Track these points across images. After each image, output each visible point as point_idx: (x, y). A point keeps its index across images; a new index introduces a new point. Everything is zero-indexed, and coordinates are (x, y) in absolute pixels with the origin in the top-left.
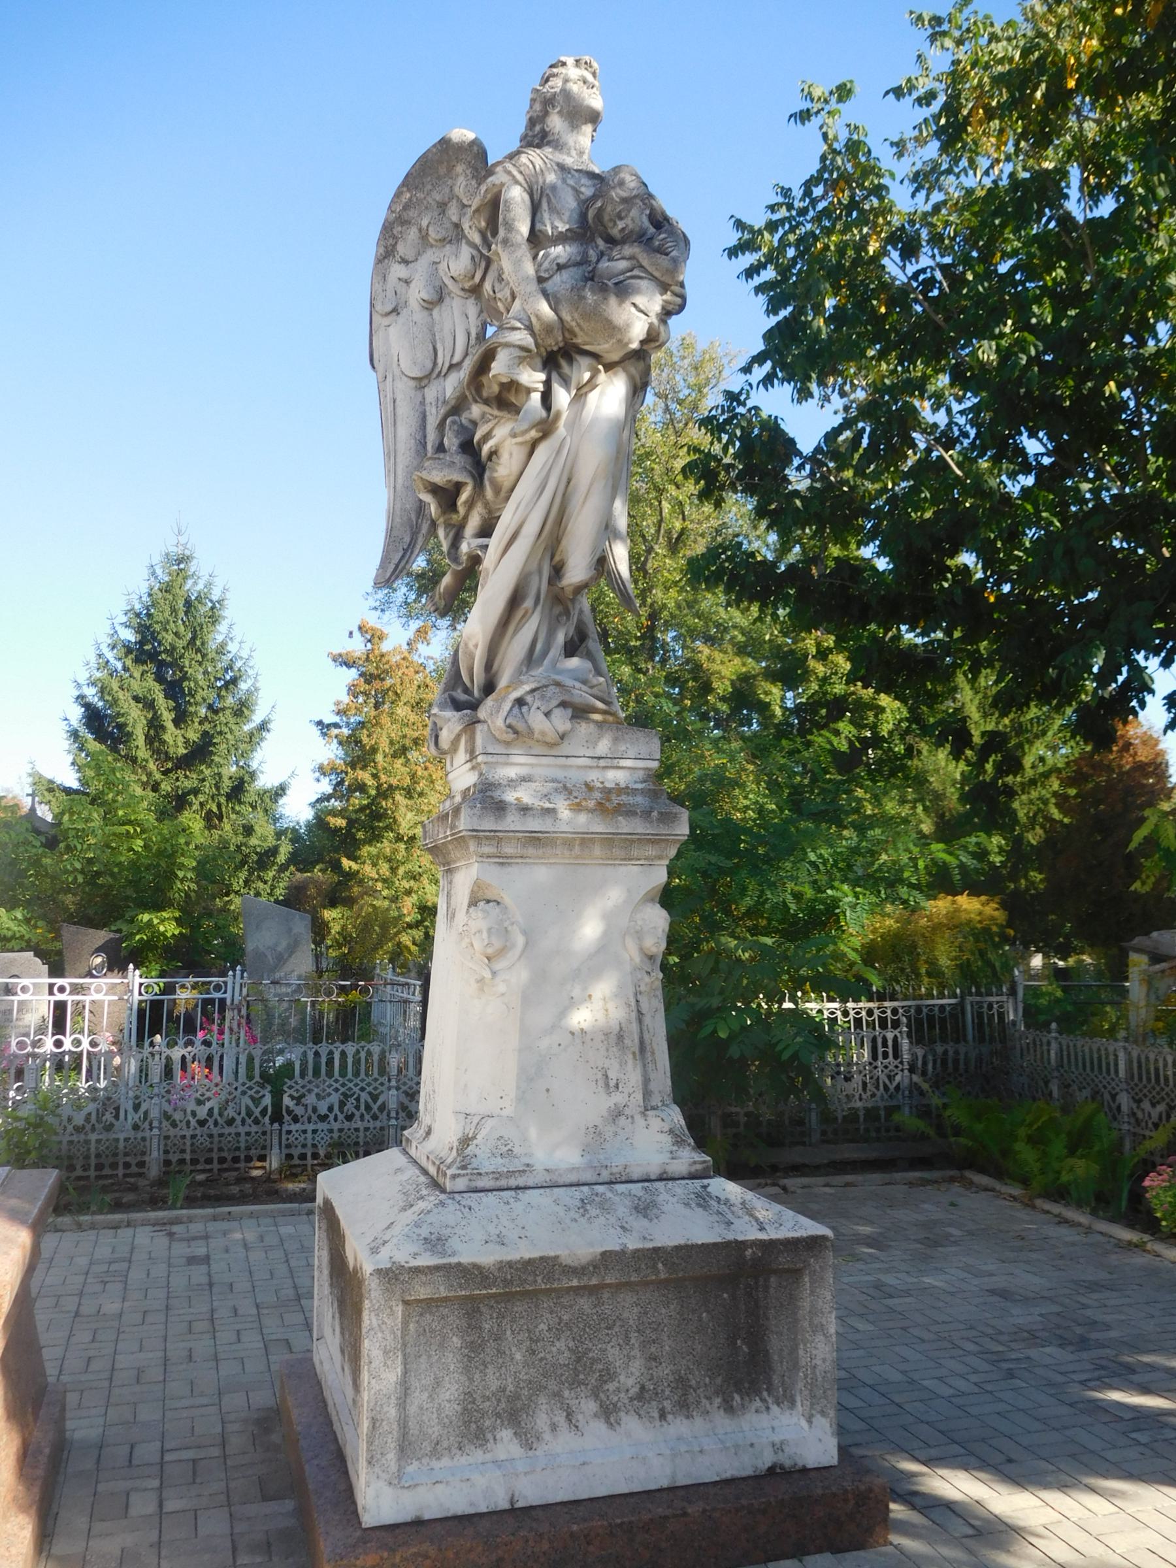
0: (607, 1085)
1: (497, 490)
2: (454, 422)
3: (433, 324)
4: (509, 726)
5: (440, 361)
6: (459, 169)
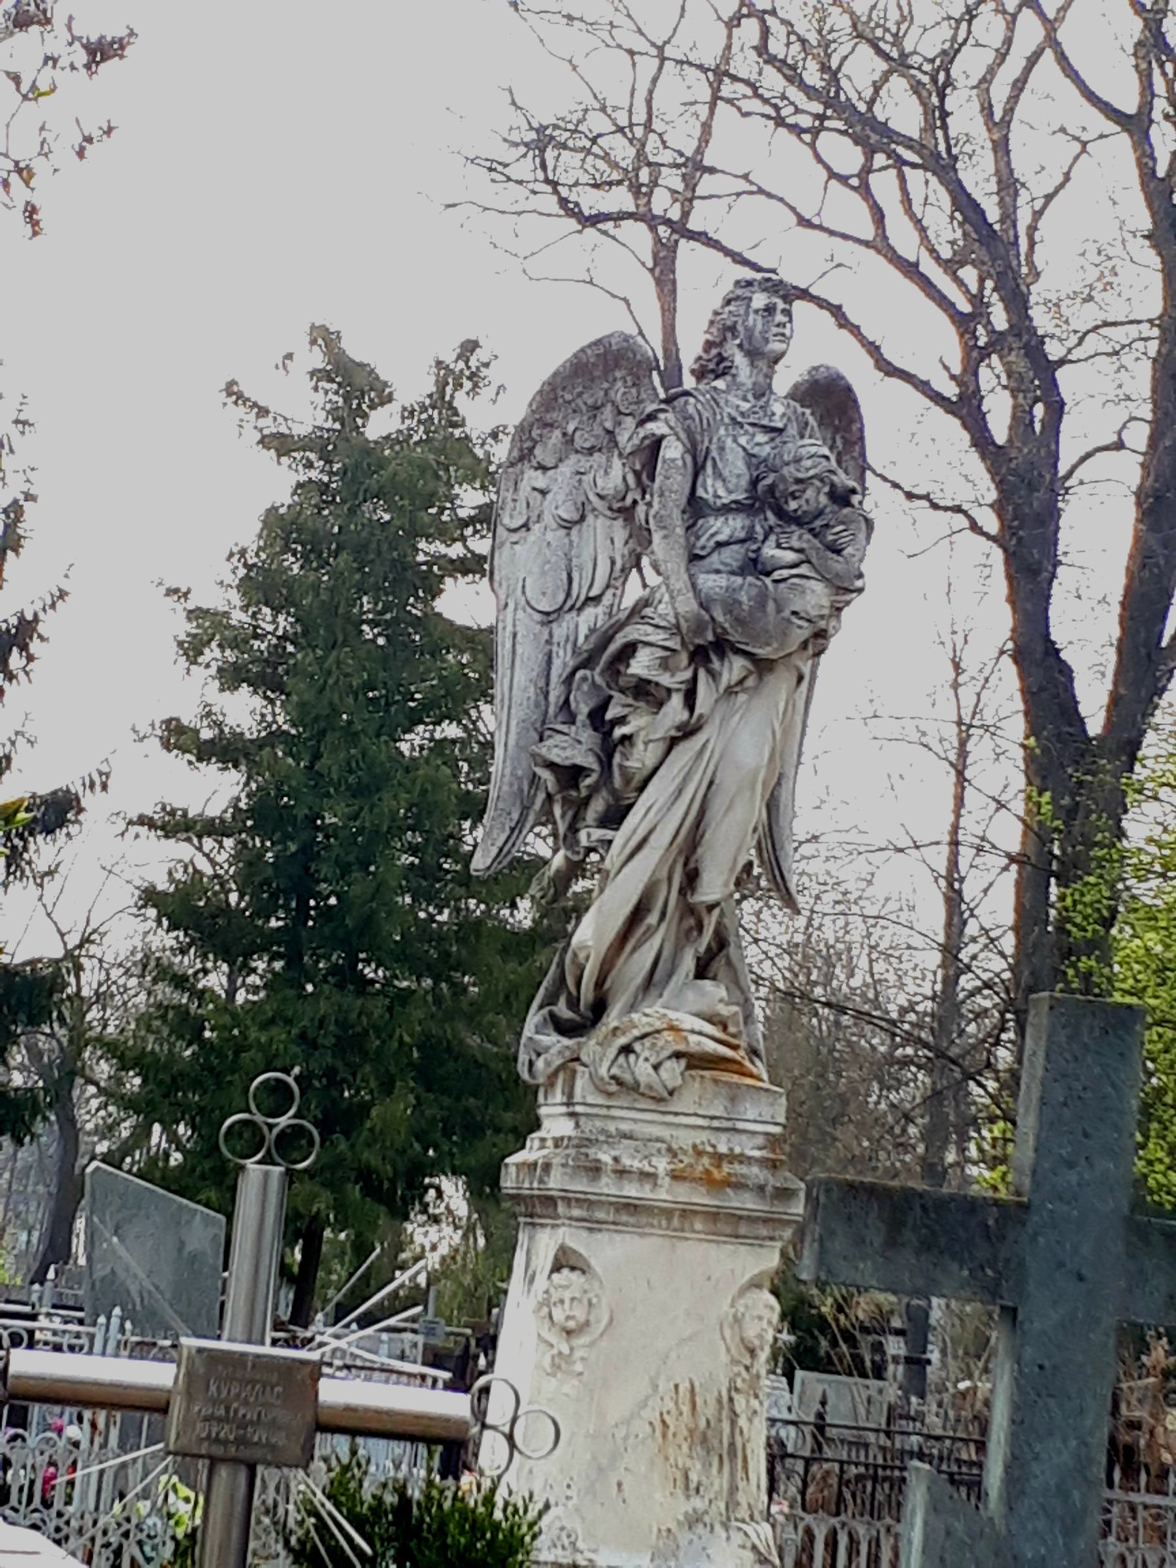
0: (687, 1488)
1: (627, 779)
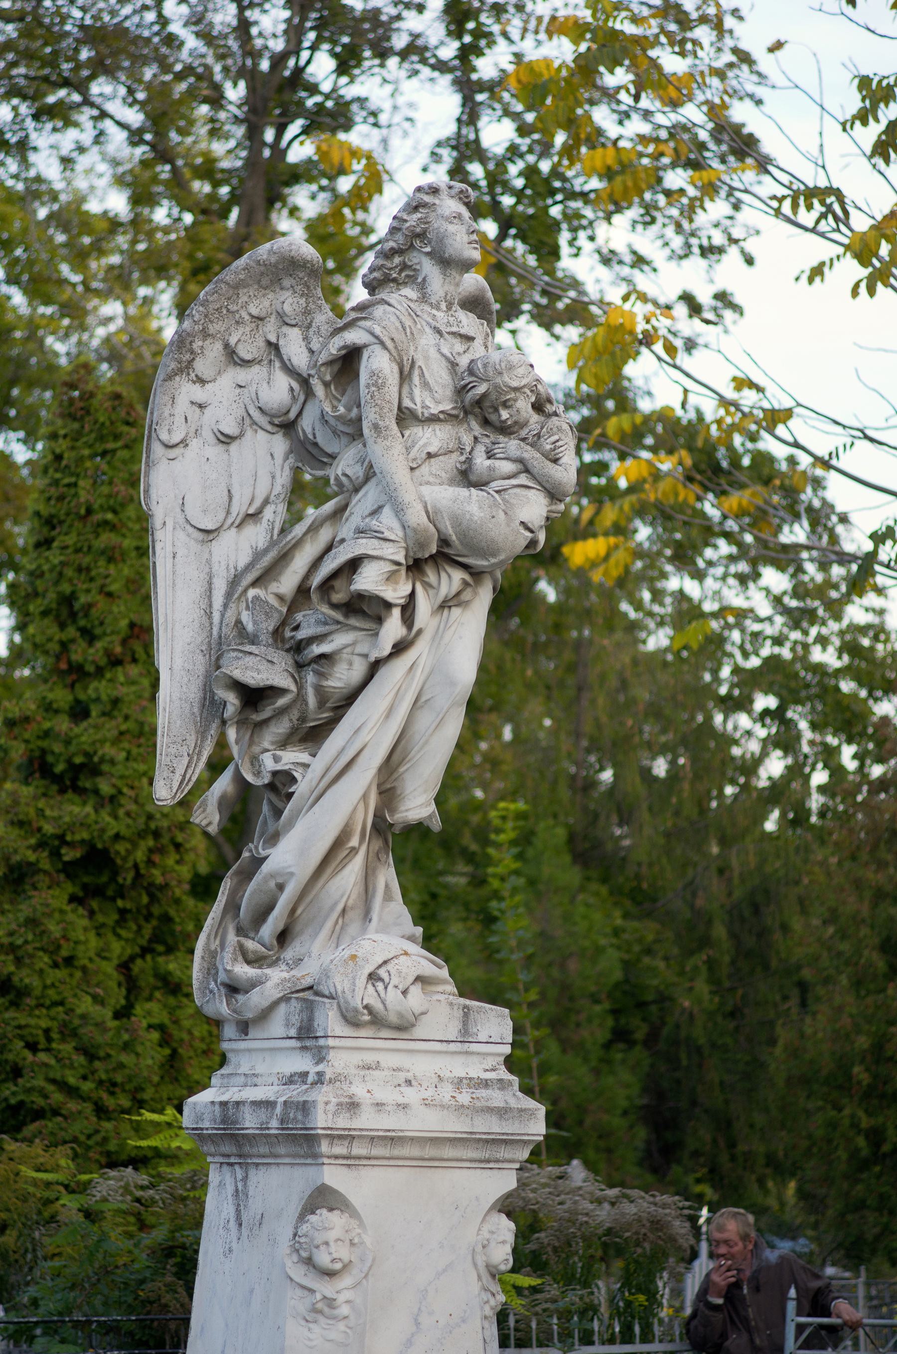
2: (256, 598)
3: (229, 466)
4: (366, 1007)
5: (234, 510)
6: (287, 282)
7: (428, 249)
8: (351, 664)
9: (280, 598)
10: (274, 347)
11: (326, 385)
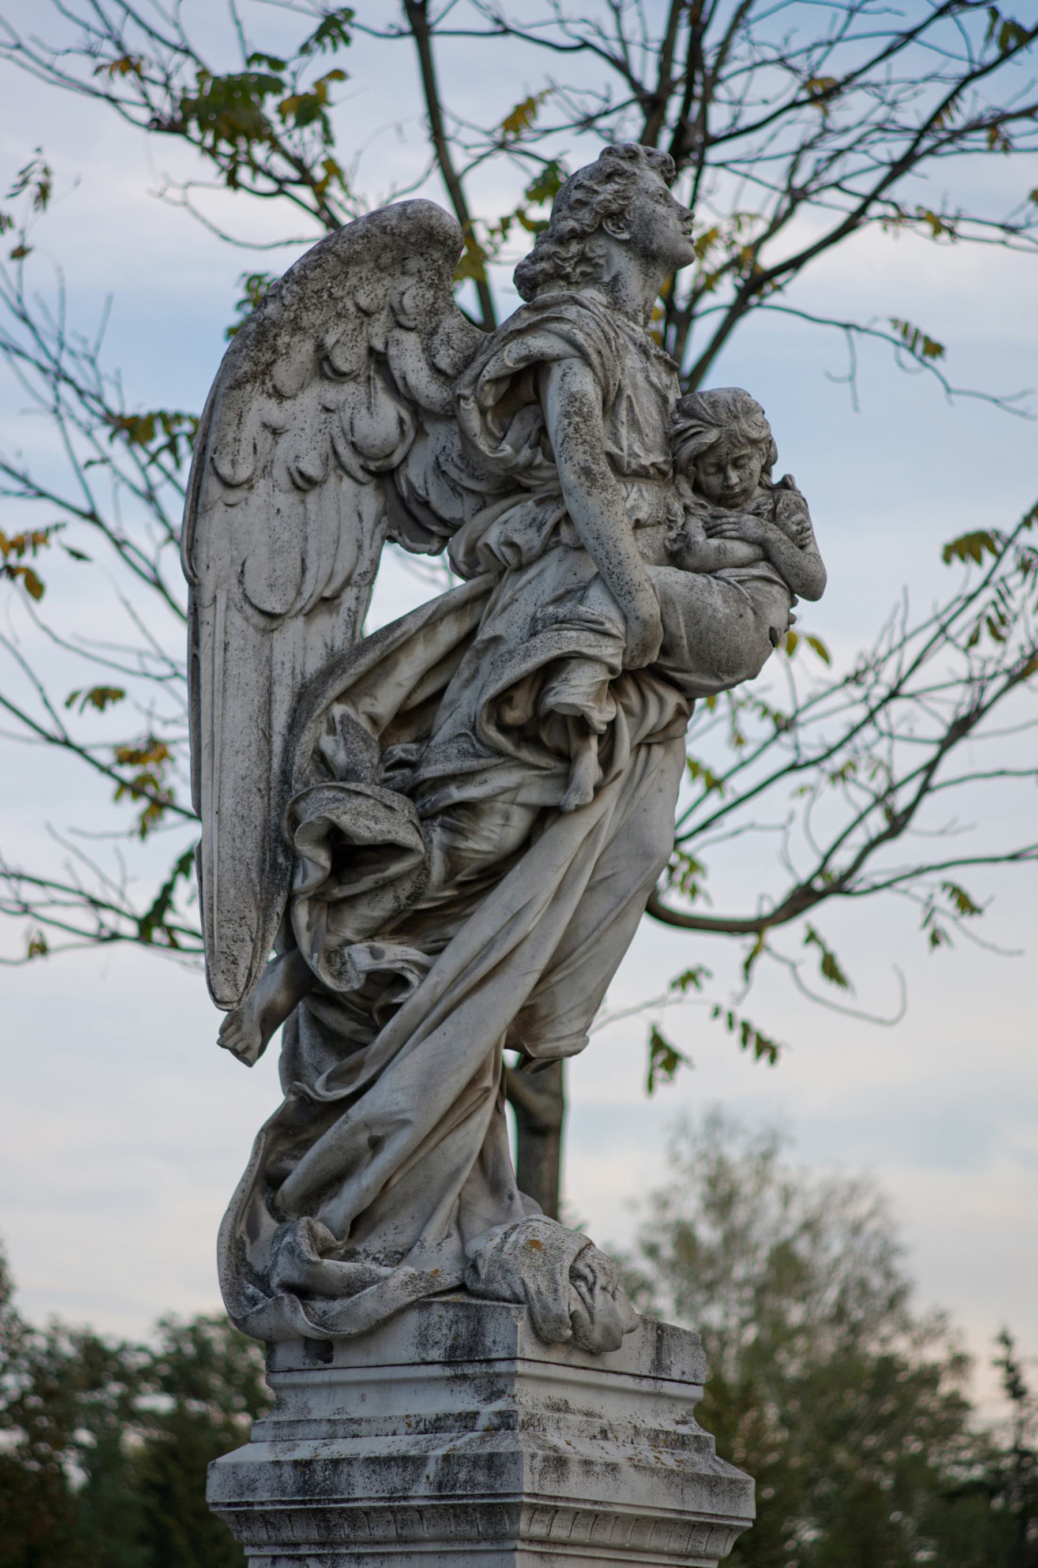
2: (345, 718)
5: (308, 589)
6: (413, 264)
7: (625, 236)
8: (507, 817)
9: (373, 720)
10: (379, 359)
11: (483, 412)
